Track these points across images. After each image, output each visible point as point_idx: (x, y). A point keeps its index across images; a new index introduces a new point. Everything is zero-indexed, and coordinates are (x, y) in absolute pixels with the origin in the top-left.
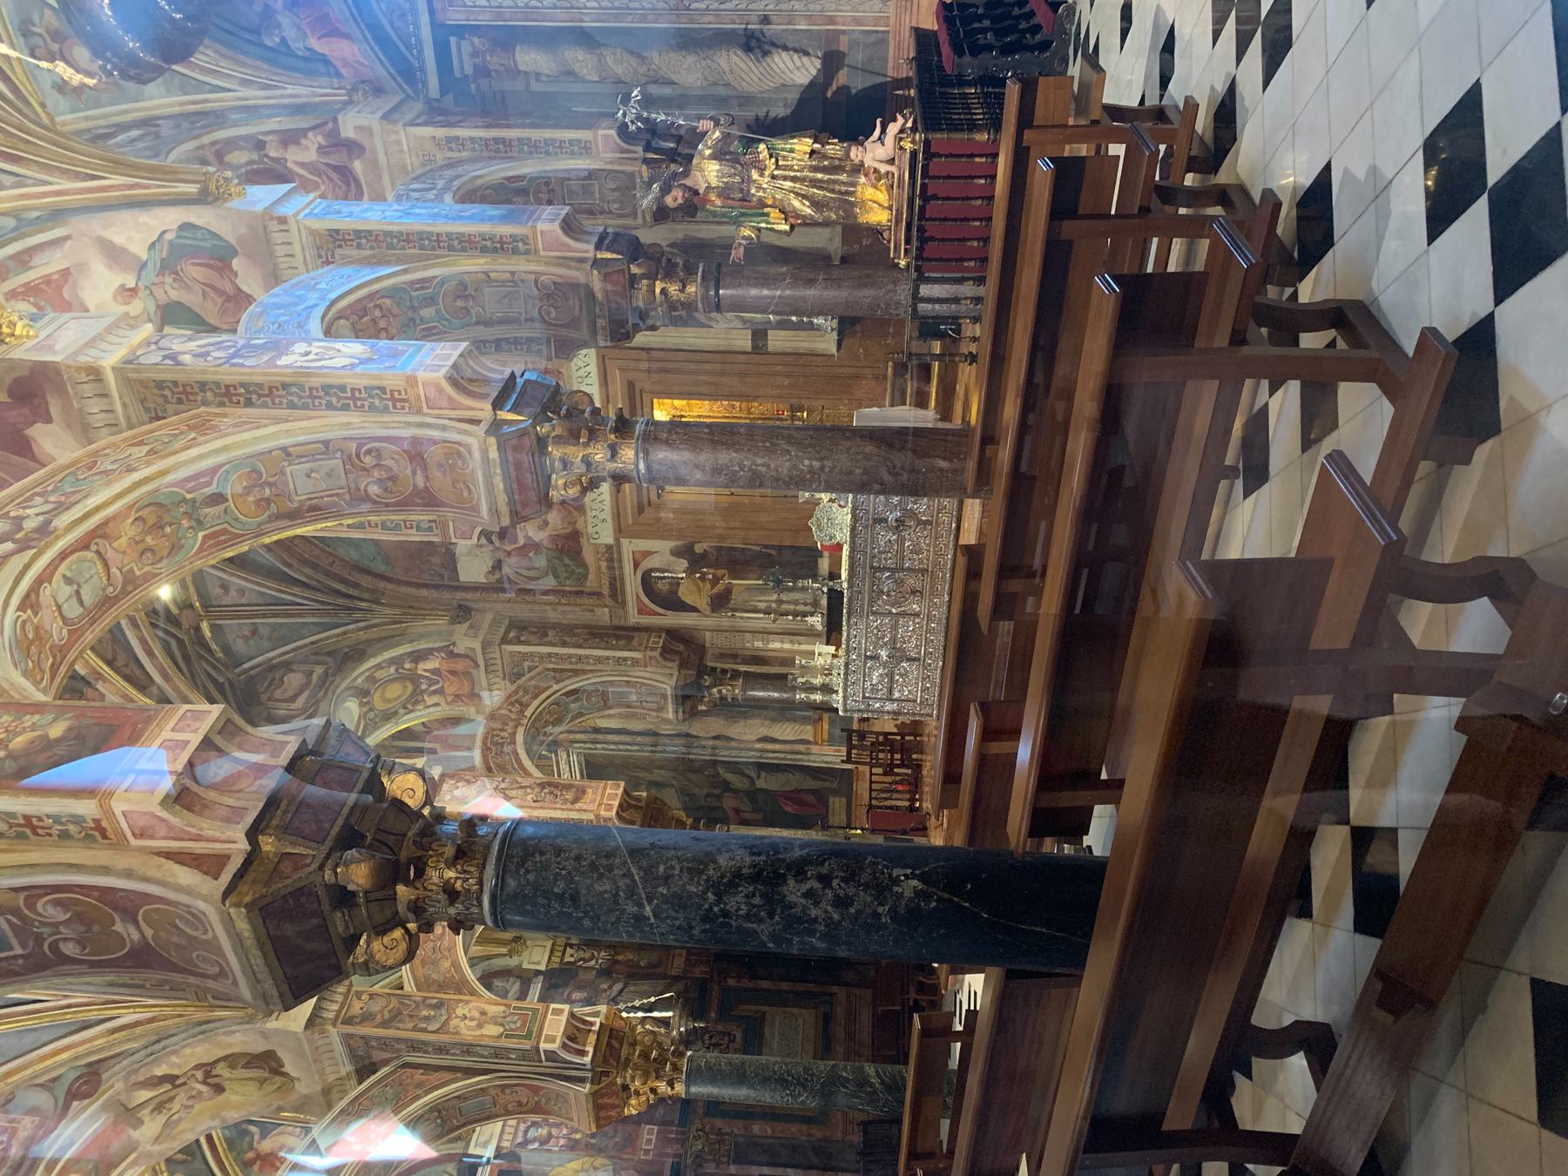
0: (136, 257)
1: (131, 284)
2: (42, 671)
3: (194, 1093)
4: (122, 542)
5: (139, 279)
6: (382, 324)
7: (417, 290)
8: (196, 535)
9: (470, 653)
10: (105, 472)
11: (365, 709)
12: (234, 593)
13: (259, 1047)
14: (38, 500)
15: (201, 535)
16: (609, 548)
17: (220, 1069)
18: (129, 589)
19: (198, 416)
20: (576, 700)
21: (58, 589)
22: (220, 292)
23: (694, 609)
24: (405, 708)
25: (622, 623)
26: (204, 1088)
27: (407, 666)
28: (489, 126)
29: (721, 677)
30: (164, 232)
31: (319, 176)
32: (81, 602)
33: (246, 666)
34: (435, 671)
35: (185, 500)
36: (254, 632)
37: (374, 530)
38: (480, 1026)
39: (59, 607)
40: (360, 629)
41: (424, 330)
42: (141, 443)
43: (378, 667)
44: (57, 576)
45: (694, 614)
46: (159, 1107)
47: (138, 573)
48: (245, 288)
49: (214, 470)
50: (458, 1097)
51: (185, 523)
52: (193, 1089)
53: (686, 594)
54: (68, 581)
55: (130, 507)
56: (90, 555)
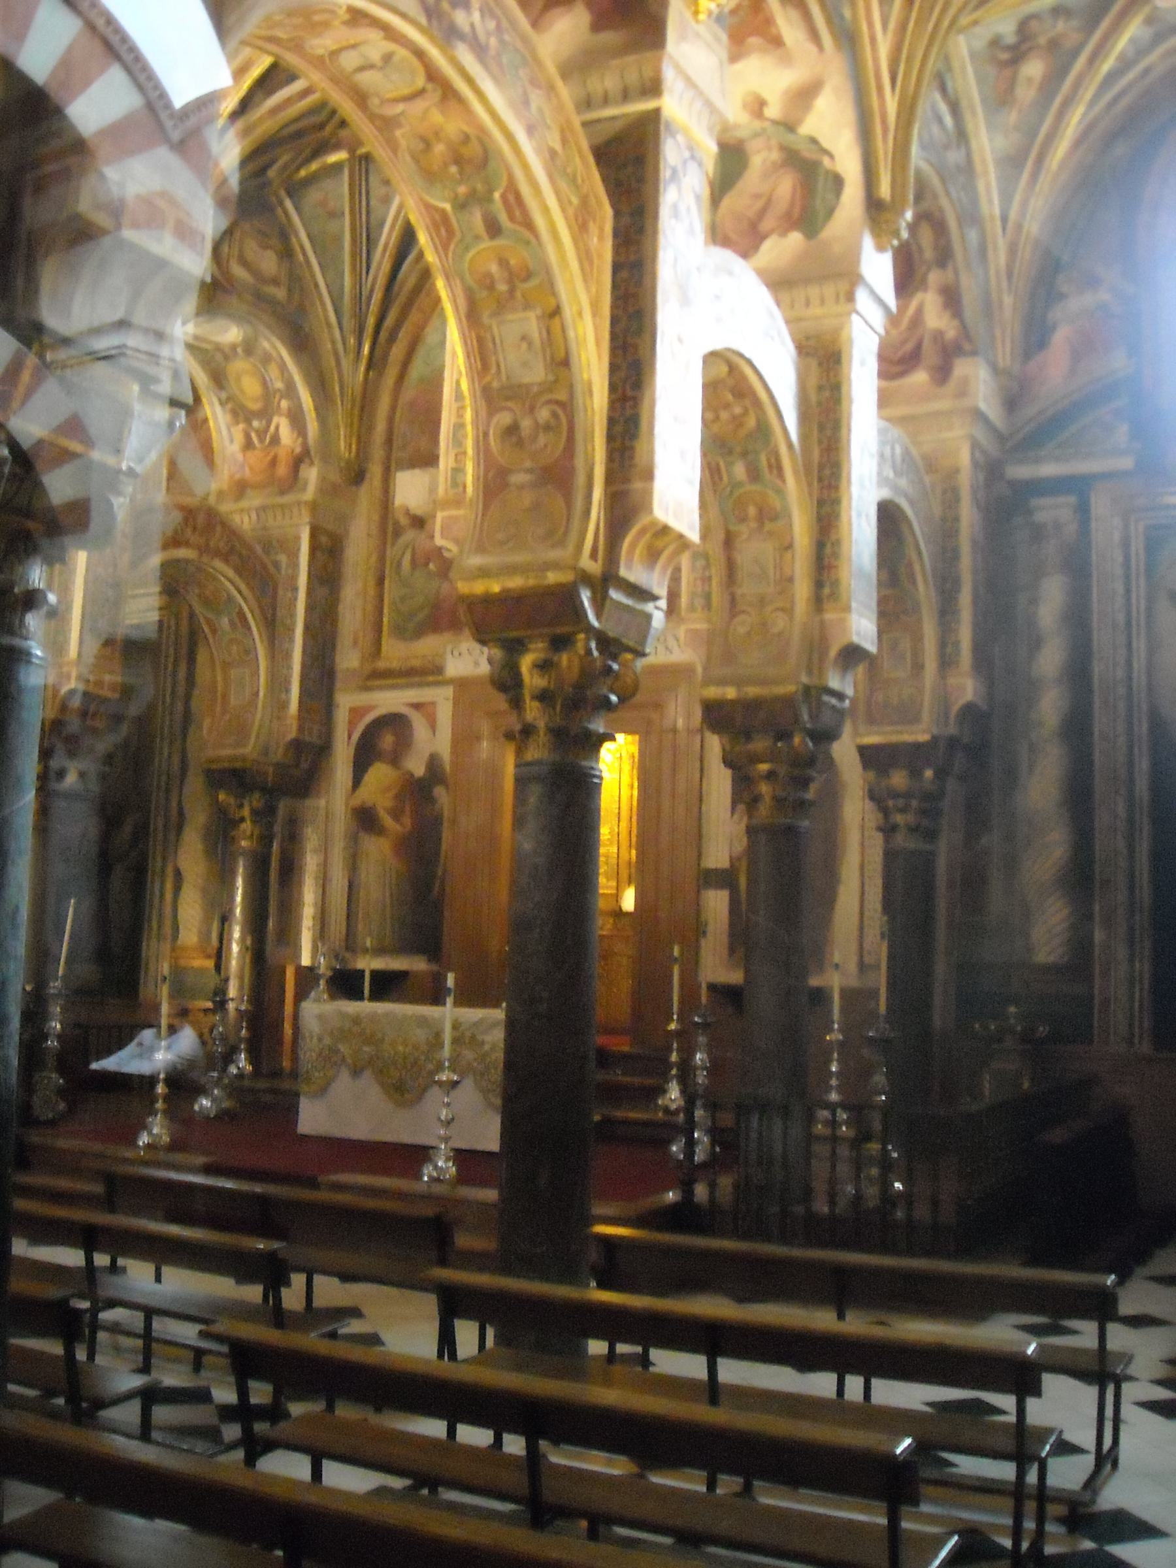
0: (800, 121)
2: (271, 28)
4: (437, 117)
5: (775, 123)
6: (724, 415)
7: (768, 460)
8: (445, 200)
10: (526, 102)
11: (227, 350)
14: (492, 25)
15: (447, 207)
16: (439, 670)
18: (378, 123)
19: (599, 203)
20: (232, 624)
21: (375, 46)
23: (357, 782)
24: (229, 399)
27: (284, 404)
28: (974, 543)
29: (265, 815)
30: (831, 156)
32: (361, 69)
33: (288, 204)
34: (276, 440)
35: (490, 191)
37: (454, 412)
39: (354, 46)
40: (333, 342)
41: (718, 464)
42: (564, 141)
43: (283, 367)
44: (391, 46)
45: (350, 784)
47: (398, 133)
48: (767, 245)
49: (529, 225)
51: (462, 190)
53: (379, 775)
54: (388, 58)
55: (482, 129)
56: (420, 81)
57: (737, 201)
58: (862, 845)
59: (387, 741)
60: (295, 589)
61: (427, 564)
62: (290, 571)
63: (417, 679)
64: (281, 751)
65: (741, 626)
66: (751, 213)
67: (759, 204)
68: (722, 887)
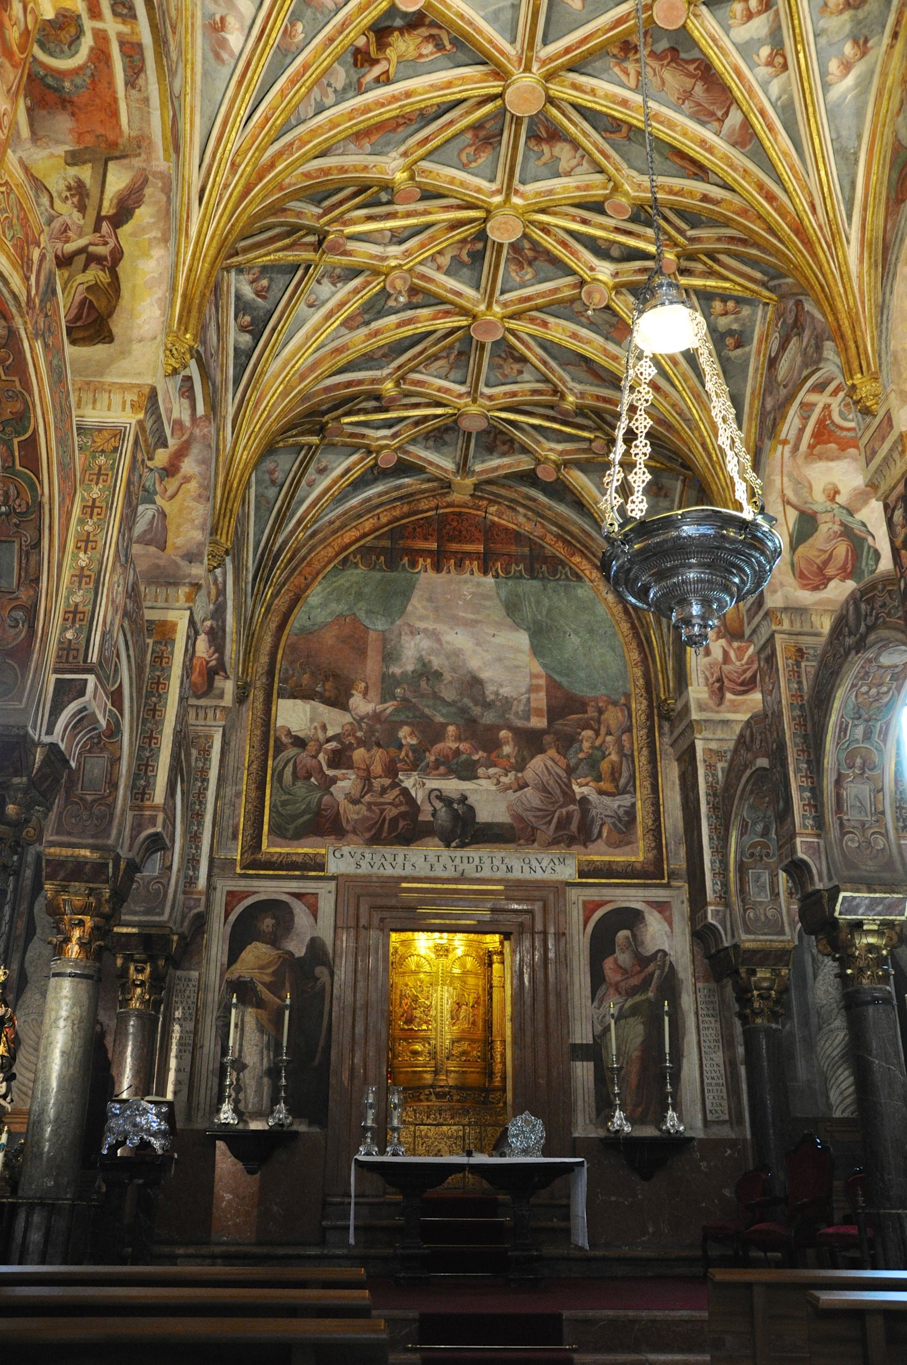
0: (858, 510)
1: (840, 499)
3: (70, 234)
5: (841, 506)
9: (216, 692)
12: (313, 477)
13: (117, 325)
17: (95, 274)
22: (826, 563)
23: (233, 958)
25: (216, 871)
26: (70, 247)
31: (747, 663)
36: (273, 482)
38: (113, 601)
41: (847, 725)
46: (79, 190)
48: (832, 584)
50: (37, 545)
52: (80, 236)
57: (808, 550)
58: (698, 1027)
59: (268, 923)
60: (205, 780)
61: (308, 778)
62: (201, 765)
63: (297, 873)
64: (186, 924)
65: (851, 842)
66: (818, 561)
67: (825, 556)
68: (588, 1060)
